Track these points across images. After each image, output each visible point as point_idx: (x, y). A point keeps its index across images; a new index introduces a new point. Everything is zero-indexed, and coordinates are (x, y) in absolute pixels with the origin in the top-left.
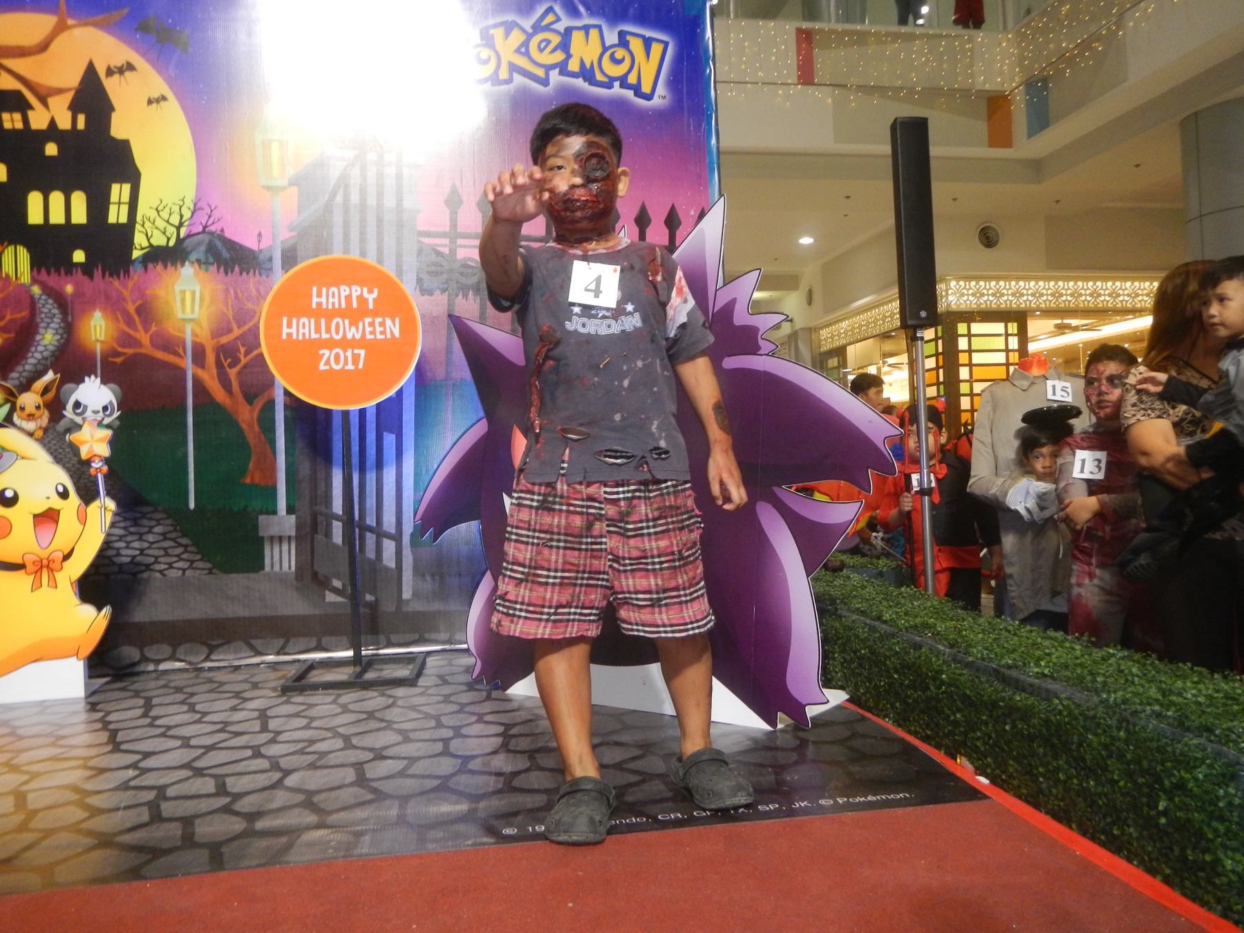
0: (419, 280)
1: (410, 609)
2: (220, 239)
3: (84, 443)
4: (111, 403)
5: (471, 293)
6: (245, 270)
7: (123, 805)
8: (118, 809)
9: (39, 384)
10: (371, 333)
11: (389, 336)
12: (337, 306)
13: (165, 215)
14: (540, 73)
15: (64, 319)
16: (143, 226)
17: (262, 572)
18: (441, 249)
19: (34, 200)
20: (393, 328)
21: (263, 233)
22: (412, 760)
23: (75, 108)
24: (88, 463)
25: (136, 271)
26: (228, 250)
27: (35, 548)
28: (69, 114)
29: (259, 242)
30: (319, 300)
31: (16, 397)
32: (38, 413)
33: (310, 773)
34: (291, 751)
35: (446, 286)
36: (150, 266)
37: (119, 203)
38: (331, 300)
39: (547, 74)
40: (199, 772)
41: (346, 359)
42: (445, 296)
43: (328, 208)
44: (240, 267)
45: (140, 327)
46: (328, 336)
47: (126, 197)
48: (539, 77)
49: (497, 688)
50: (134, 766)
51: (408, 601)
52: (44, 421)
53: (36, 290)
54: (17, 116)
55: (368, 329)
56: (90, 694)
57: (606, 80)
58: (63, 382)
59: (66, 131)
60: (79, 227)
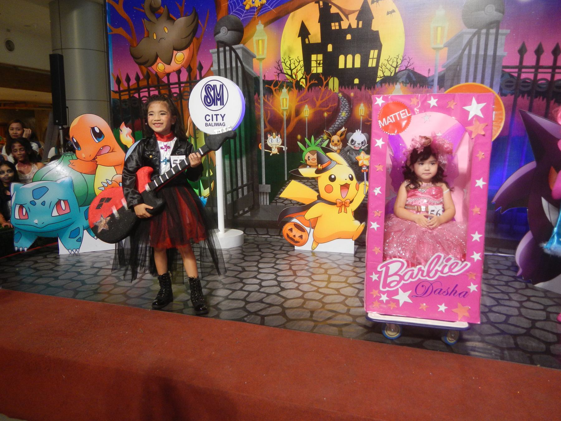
0: (501, 89)
2: (412, 73)
3: (360, 160)
4: (365, 141)
5: (526, 95)
6: (422, 85)
9: (339, 132)
13: (390, 63)
15: (350, 107)
16: (381, 68)
18: (513, 74)
19: (342, 58)
21: (430, 69)
22: (508, 316)
23: (358, 19)
24: (361, 167)
25: (378, 86)
26: (415, 78)
27: (341, 198)
28: (356, 21)
29: (429, 73)
31: (331, 137)
32: (338, 144)
35: (513, 92)
36: (383, 84)
37: (373, 58)
42: (513, 96)
43: (461, 57)
47: (376, 56)
49: (530, 282)
52: (340, 147)
53: (340, 95)
54: (337, 24)
56: (356, 253)
58: (348, 132)
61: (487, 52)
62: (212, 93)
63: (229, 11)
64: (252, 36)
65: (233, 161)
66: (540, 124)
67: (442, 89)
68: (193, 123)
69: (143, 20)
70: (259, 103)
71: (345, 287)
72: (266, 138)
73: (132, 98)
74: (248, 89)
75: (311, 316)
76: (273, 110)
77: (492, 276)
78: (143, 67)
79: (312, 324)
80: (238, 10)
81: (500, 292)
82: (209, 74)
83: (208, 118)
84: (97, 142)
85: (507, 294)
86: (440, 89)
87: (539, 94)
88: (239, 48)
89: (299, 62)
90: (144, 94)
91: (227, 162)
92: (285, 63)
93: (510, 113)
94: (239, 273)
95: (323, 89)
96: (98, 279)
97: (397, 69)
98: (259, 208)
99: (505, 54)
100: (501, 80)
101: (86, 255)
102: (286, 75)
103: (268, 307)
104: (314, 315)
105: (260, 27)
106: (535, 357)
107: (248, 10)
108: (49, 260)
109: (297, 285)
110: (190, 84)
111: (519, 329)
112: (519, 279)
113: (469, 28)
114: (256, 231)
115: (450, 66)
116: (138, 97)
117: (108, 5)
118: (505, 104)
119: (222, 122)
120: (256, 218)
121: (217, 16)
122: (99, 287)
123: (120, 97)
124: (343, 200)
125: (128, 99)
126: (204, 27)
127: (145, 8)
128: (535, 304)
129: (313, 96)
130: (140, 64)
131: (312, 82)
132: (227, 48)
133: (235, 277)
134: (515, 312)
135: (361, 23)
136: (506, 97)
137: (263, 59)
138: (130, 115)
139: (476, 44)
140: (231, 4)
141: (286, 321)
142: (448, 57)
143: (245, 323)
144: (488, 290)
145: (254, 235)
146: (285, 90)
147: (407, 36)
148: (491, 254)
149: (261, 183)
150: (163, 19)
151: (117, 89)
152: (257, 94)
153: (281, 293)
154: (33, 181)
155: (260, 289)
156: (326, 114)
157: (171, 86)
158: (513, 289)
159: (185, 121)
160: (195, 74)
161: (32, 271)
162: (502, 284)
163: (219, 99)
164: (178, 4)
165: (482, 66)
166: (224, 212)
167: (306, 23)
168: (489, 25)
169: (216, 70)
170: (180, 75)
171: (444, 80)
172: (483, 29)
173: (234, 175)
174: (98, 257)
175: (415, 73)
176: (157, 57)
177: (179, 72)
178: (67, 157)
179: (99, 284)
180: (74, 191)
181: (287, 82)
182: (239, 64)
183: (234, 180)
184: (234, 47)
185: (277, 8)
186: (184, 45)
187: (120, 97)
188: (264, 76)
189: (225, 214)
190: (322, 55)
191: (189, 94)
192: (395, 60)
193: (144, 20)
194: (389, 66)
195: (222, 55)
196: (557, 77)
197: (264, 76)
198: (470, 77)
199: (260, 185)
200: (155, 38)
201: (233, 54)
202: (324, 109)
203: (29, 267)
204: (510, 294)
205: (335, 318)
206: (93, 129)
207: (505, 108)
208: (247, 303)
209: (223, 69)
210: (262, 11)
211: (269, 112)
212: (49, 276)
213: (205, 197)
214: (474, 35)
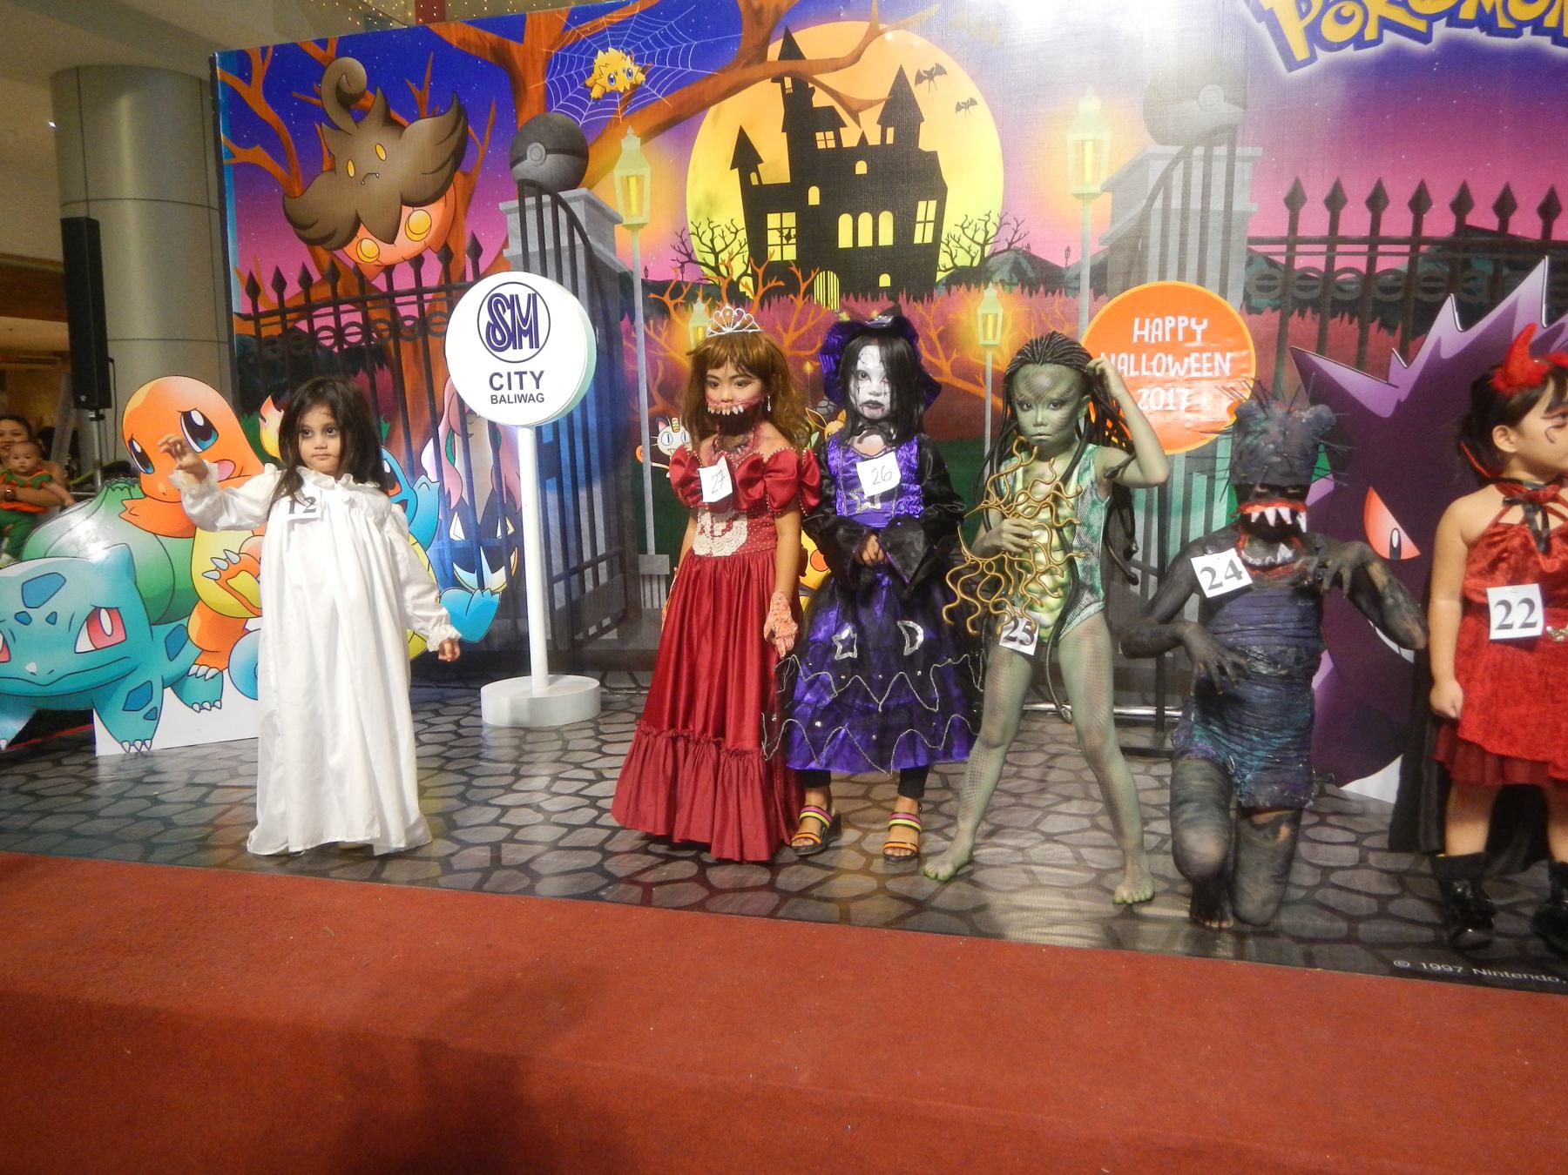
0: (1247, 297)
2: (1026, 257)
5: (1309, 310)
8: (994, 866)
10: (1199, 370)
11: (1217, 373)
12: (1160, 339)
13: (970, 232)
14: (1420, 26)
16: (947, 245)
18: (1276, 258)
19: (845, 221)
20: (1224, 362)
23: (884, 122)
25: (940, 292)
26: (1033, 268)
28: (879, 127)
29: (1067, 257)
30: (1142, 333)
35: (1278, 302)
36: (954, 288)
37: (925, 222)
38: (1154, 333)
39: (1430, 27)
40: (1050, 838)
41: (1167, 396)
42: (1278, 313)
43: (1144, 218)
44: (1045, 287)
45: (941, 354)
46: (1148, 373)
47: (931, 216)
48: (1423, 33)
49: (1331, 781)
54: (830, 135)
55: (1194, 365)
57: (1511, 26)
62: (507, 316)
64: (611, 165)
65: (568, 496)
66: (1338, 380)
67: (1103, 297)
68: (459, 396)
69: (317, 126)
70: (634, 342)
71: (864, 809)
72: (654, 432)
73: (290, 333)
74: (604, 304)
76: (672, 359)
78: (319, 250)
79: (771, 900)
80: (571, 100)
82: (499, 265)
83: (497, 382)
86: (1096, 299)
87: (1339, 307)
88: (576, 199)
89: (736, 234)
90: (324, 320)
91: (552, 498)
92: (698, 235)
93: (1272, 357)
94: (587, 784)
95: (799, 302)
96: (207, 813)
97: (988, 250)
98: (641, 617)
99: (1255, 207)
101: (169, 753)
102: (704, 268)
103: (664, 863)
105: (630, 143)
106: (1315, 949)
107: (598, 99)
108: (69, 770)
110: (449, 293)
113: (1163, 144)
114: (635, 680)
115: (1119, 239)
116: (307, 331)
117: (223, 90)
119: (535, 392)
120: (631, 646)
122: (213, 832)
123: (258, 331)
125: (280, 335)
126: (482, 144)
127: (323, 97)
129: (774, 320)
130: (311, 243)
131: (769, 285)
132: (546, 199)
133: (577, 794)
135: (890, 132)
137: (641, 226)
138: (285, 380)
139: (1181, 184)
140: (552, 83)
141: (706, 893)
142: (1112, 217)
143: (601, 903)
145: (628, 689)
146: (700, 307)
147: (1008, 164)
149: (644, 550)
150: (373, 122)
151: (249, 310)
152: (627, 316)
154: (24, 557)
156: (808, 367)
157: (398, 300)
161: (24, 800)
163: (525, 333)
164: (412, 86)
165: (1198, 238)
166: (546, 631)
168: (1210, 138)
169: (517, 256)
171: (1106, 274)
173: (571, 531)
174: (204, 758)
175: (1033, 259)
176: (357, 222)
177: (417, 261)
178: (114, 496)
179: (210, 823)
180: (136, 584)
181: (704, 285)
182: (578, 241)
183: (572, 545)
184: (562, 194)
185: (676, 93)
186: (429, 193)
187: (258, 331)
188: (646, 270)
189: (550, 637)
190: (794, 214)
191: (445, 320)
192: (981, 225)
193: (321, 126)
194: (965, 242)
195: (531, 216)
196: (1383, 264)
197: (646, 270)
198: (1169, 266)
199: (640, 556)
200: (352, 174)
201: (562, 215)
202: (803, 353)
203: (15, 790)
205: (833, 881)
206: (187, 416)
207: (1258, 347)
208: (607, 855)
209: (534, 253)
210: (635, 102)
211: (660, 363)
212: (73, 810)
213: (493, 593)
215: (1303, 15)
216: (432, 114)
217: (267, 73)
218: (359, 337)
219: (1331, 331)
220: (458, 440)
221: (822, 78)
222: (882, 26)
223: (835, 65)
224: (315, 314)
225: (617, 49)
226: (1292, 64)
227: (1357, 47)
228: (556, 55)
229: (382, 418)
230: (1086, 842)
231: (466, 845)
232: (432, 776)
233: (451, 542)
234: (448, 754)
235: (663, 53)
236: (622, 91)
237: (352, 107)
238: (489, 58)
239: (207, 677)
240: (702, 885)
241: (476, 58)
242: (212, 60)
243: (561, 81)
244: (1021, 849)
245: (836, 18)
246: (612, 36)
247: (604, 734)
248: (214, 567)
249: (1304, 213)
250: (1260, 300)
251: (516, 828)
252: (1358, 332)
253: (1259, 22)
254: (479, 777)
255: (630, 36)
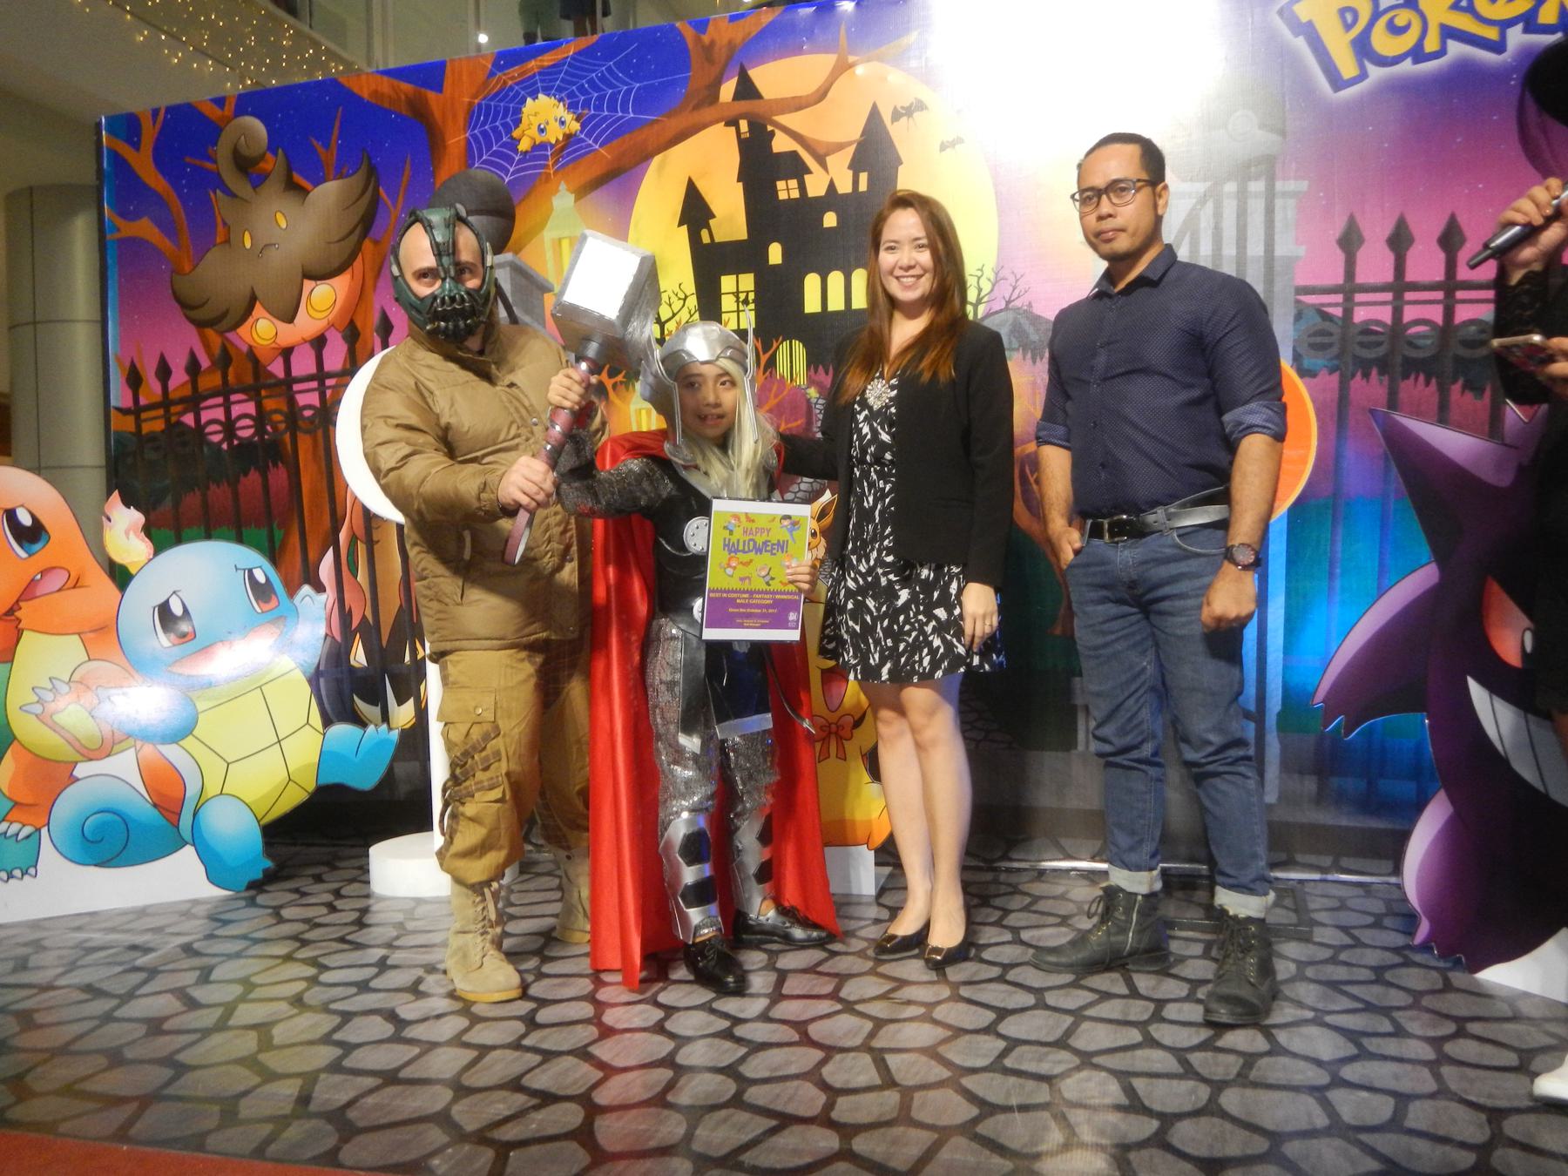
1: (1276, 819)
5: (1374, 372)
7: (1014, 1101)
8: (1007, 1109)
14: (1492, 34)
17: (1073, 752)
19: (812, 282)
22: (1403, 1099)
23: (856, 166)
26: (1037, 330)
28: (850, 173)
32: (815, 542)
33: (1249, 1092)
34: (1196, 1040)
35: (1336, 362)
39: (1503, 36)
40: (1087, 1060)
42: (1338, 373)
50: (990, 1030)
51: (1270, 807)
53: (813, 393)
54: (793, 183)
59: (846, 196)
60: (856, 311)
61: (1245, 247)
63: (469, 158)
64: (542, 225)
69: (212, 195)
71: (828, 1016)
73: (174, 428)
75: (689, 1137)
77: (1328, 953)
78: (210, 332)
80: (495, 154)
81: (1360, 1006)
84: (23, 554)
85: (1386, 1011)
87: (1412, 367)
89: (685, 300)
90: (213, 413)
99: (1301, 251)
100: (1295, 330)
103: (536, 1108)
104: (698, 1132)
105: (563, 200)
107: (526, 152)
109: (659, 1014)
111: (1447, 1148)
112: (1418, 958)
118: (1314, 401)
121: (433, 174)
123: (138, 427)
124: (833, 718)
125: (163, 431)
126: (395, 207)
127: (220, 161)
128: (1489, 1049)
130: (200, 325)
134: (1423, 1081)
135: (863, 177)
136: (1315, 380)
138: (167, 482)
140: (475, 137)
144: (1320, 1006)
148: (1316, 876)
150: (272, 187)
151: (129, 403)
153: (598, 1051)
155: (524, 1036)
157: (296, 387)
158: (1401, 994)
159: (337, 490)
160: (370, 347)
162: (1361, 978)
167: (701, 186)
168: (1244, 171)
170: (326, 352)
172: (1229, 180)
176: (253, 300)
177: (319, 342)
185: (615, 143)
186: (336, 264)
187: (138, 427)
196: (1463, 314)
200: (248, 244)
204: (1396, 1014)
206: (11, 515)
210: (569, 154)
214: (1203, 200)
215: (1348, 27)
216: (339, 175)
217: (158, 139)
218: (250, 432)
219: (1403, 395)
220: (361, 547)
221: (782, 119)
222: (851, 59)
223: (798, 104)
224: (202, 405)
225: (548, 95)
226: (1337, 82)
227: (1416, 61)
228: (480, 105)
229: (275, 526)
230: (1140, 1066)
231: (271, 1076)
232: (268, 969)
233: (352, 670)
234: (307, 936)
235: (601, 99)
236: (553, 142)
237: (250, 170)
238: (404, 113)
239: (20, 837)
240: (583, 1145)
241: (388, 112)
242: (99, 124)
243: (484, 133)
244: (1047, 1079)
245: (798, 51)
246: (542, 81)
247: (512, 905)
248: (36, 699)
249: (1362, 255)
250: (1312, 361)
251: (348, 1048)
252: (1437, 395)
253: (1296, 35)
254: (334, 968)
255: (563, 80)
